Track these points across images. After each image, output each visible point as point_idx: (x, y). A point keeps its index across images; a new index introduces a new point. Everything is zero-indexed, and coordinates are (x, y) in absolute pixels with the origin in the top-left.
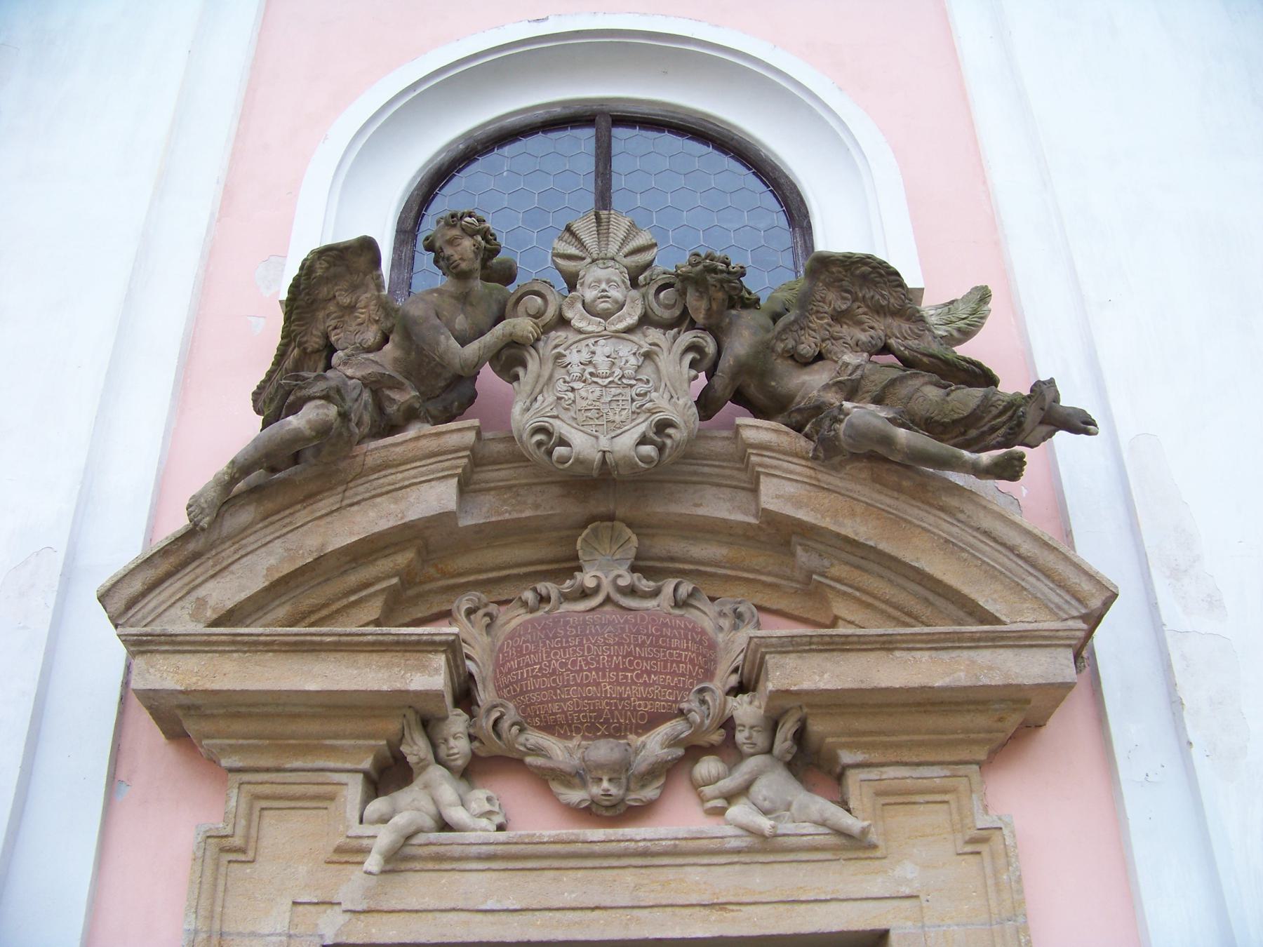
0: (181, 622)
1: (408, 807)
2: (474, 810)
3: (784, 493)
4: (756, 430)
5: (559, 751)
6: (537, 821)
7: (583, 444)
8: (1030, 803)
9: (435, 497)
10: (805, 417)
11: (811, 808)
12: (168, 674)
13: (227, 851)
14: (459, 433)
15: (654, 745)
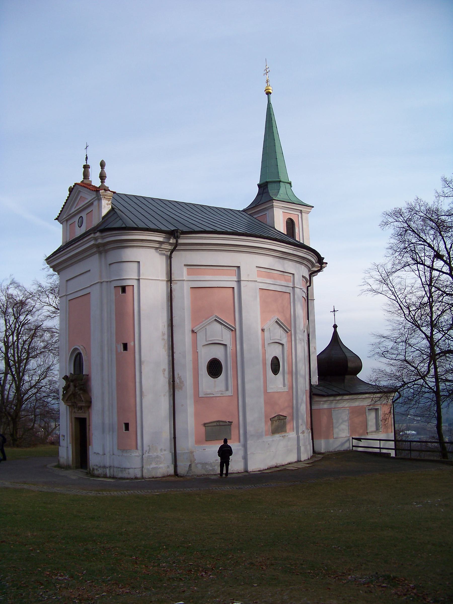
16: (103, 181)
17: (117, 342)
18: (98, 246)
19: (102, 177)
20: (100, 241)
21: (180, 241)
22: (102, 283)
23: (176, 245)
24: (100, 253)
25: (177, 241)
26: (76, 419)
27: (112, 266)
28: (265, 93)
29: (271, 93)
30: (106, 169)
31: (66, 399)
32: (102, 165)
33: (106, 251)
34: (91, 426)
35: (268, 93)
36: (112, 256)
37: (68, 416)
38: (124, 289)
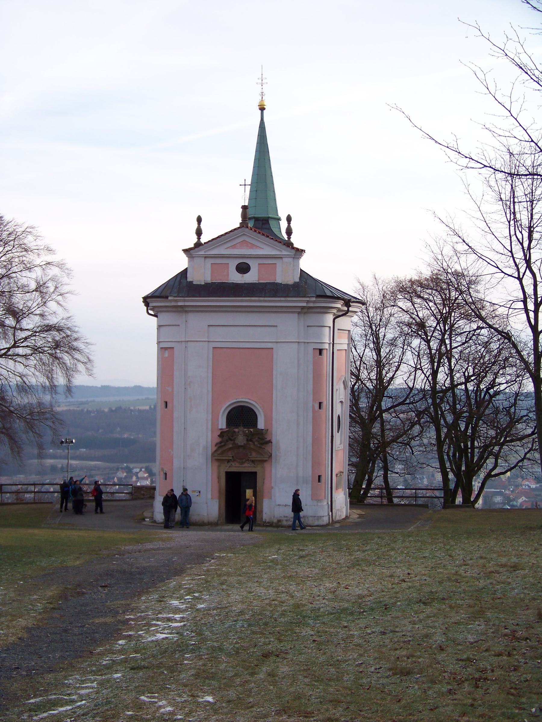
0: (216, 455)
1: (230, 464)
2: (233, 464)
3: (252, 446)
4: (250, 443)
5: (238, 460)
6: (237, 465)
7: (239, 444)
8: (266, 465)
9: (231, 446)
10: (253, 442)
11: (253, 465)
12: (216, 458)
13: (219, 466)
14: (232, 442)
15: (244, 460)
16: (289, 238)
17: (314, 400)
18: (303, 308)
19: (289, 232)
20: (311, 305)
21: (351, 309)
22: (298, 342)
23: (348, 311)
24: (299, 313)
25: (348, 309)
26: (228, 474)
27: (309, 328)
28: (258, 108)
29: (264, 109)
30: (292, 225)
31: (219, 452)
32: (289, 219)
33: (305, 313)
34: (266, 481)
35: (262, 109)
36: (312, 319)
37: (210, 471)
38: (321, 351)
